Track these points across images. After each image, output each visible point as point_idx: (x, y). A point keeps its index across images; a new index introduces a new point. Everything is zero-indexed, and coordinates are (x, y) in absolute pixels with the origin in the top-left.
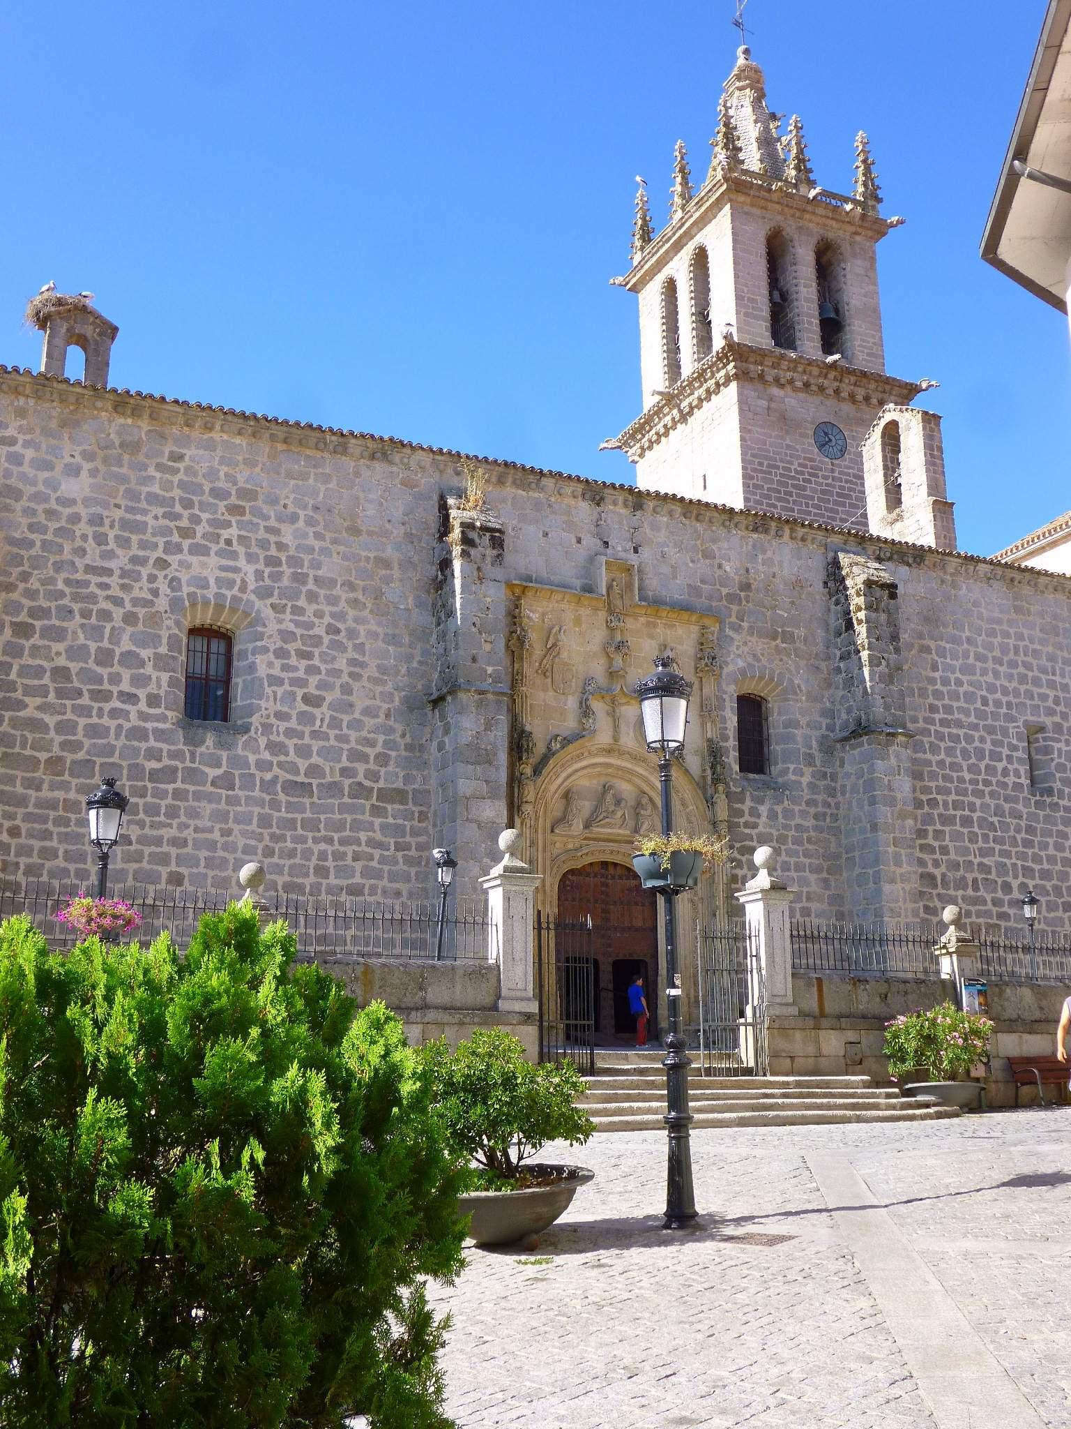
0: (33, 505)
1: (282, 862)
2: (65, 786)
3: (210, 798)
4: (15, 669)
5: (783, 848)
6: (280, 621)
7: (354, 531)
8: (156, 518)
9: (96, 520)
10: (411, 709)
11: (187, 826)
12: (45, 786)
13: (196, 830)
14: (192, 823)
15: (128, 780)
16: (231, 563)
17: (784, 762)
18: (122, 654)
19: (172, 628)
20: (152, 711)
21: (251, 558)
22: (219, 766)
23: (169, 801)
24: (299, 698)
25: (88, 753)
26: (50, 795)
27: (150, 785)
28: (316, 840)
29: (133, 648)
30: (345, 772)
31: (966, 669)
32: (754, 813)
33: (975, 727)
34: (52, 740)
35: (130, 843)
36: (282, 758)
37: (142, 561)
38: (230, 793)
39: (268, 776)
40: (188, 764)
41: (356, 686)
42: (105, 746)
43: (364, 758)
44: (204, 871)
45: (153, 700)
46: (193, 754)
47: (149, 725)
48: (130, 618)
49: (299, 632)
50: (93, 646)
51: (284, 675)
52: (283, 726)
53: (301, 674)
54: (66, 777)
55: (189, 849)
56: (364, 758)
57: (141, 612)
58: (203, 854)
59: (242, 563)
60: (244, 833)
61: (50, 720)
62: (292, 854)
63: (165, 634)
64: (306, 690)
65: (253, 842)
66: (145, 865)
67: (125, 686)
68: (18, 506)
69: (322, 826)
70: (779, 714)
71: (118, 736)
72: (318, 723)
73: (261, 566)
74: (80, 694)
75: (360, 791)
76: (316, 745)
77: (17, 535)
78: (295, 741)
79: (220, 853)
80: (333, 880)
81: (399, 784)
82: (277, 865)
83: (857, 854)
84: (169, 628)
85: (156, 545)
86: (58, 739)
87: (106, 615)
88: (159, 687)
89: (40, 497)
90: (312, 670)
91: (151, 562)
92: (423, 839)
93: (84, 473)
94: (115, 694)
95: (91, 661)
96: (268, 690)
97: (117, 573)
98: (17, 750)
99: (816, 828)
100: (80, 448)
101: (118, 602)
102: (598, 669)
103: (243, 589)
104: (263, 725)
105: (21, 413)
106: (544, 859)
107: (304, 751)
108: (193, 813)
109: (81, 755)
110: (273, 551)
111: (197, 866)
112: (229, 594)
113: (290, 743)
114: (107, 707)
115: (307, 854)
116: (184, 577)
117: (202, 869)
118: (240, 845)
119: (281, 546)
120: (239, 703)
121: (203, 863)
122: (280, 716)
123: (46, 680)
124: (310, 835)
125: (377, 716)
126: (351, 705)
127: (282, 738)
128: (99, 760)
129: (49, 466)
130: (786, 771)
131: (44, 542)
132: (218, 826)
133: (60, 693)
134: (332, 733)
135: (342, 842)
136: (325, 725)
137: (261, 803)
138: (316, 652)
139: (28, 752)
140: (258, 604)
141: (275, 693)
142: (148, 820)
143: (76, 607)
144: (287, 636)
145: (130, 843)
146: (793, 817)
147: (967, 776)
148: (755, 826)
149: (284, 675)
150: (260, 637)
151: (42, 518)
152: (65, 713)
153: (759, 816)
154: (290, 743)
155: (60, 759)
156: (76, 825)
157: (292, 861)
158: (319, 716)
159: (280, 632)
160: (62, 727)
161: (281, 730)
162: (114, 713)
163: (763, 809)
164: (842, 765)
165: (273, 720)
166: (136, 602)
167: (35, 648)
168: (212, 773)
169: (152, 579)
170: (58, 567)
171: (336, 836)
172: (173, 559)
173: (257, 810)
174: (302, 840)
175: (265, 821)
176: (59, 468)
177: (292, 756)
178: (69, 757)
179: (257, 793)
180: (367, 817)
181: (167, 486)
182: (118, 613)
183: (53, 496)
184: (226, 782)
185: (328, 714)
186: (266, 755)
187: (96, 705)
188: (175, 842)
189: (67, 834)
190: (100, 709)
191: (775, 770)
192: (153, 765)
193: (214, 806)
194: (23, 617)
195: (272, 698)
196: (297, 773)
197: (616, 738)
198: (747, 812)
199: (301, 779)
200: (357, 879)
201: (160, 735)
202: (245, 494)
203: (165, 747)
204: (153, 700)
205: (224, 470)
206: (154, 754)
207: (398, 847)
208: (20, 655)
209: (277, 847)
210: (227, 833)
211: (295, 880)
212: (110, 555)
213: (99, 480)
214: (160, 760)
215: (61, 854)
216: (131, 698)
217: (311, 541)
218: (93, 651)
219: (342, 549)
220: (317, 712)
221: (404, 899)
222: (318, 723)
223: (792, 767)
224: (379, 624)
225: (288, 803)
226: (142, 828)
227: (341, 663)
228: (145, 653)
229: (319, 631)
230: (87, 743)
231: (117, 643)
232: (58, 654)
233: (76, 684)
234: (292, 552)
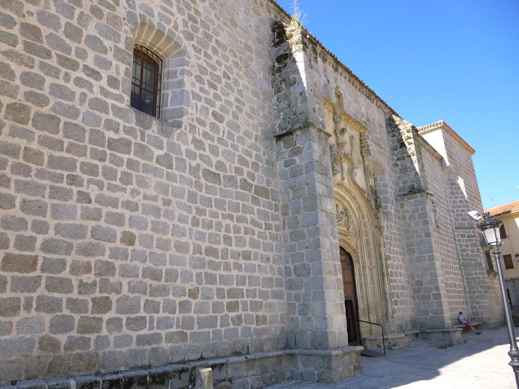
1: (204, 231)
2: (28, 135)
3: (156, 172)
6: (199, 59)
7: (235, 25)
10: (267, 138)
11: (138, 193)
13: (145, 197)
14: (142, 190)
15: (90, 142)
16: (168, 7)
18: (88, 36)
22: (162, 149)
23: (124, 168)
24: (210, 113)
25: (53, 109)
26: (10, 140)
27: (108, 152)
29: (98, 36)
34: (17, 87)
35: (90, 202)
38: (169, 170)
39: (194, 164)
40: (139, 141)
41: (240, 115)
42: (70, 107)
43: (246, 163)
44: (151, 233)
45: (113, 82)
46: (143, 134)
47: (110, 101)
49: (209, 70)
52: (202, 129)
54: (29, 126)
55: (139, 213)
58: (150, 218)
59: (174, 10)
60: (180, 205)
61: (18, 69)
62: (209, 226)
64: (214, 109)
65: (185, 213)
66: (102, 223)
67: (90, 62)
69: (226, 207)
70: (381, 180)
72: (221, 133)
74: (49, 55)
75: (246, 185)
76: (221, 148)
78: (209, 142)
79: (163, 219)
80: (234, 248)
81: (264, 185)
82: (201, 233)
84: (126, 32)
86: (24, 89)
88: (118, 73)
94: (81, 67)
96: (192, 101)
103: (176, 27)
104: (190, 125)
107: (214, 150)
108: (142, 183)
109: (46, 110)
111: (146, 228)
112: (167, 27)
113: (207, 143)
114: (74, 74)
115: (219, 226)
117: (149, 232)
118: (177, 215)
120: (169, 107)
121: (150, 225)
122: (202, 123)
127: (201, 138)
132: (160, 196)
135: (239, 220)
136: (225, 136)
137: (190, 183)
140: (185, 42)
141: (197, 105)
142: (106, 182)
145: (90, 202)
150: (186, 63)
152: (32, 67)
154: (207, 143)
155: (24, 108)
156: (37, 175)
157: (210, 231)
158: (221, 128)
161: (201, 132)
162: (79, 81)
165: (195, 123)
168: (157, 152)
173: (187, 188)
175: (192, 198)
177: (207, 153)
178: (34, 109)
179: (187, 175)
186: (192, 147)
187: (64, 70)
188: (128, 205)
189: (26, 183)
192: (110, 134)
193: (158, 179)
195: (195, 108)
196: (211, 166)
199: (213, 169)
200: (247, 248)
201: (117, 111)
203: (122, 122)
204: (113, 82)
206: (111, 126)
209: (201, 218)
210: (167, 203)
211: (213, 245)
214: (117, 132)
215: (18, 202)
216: (96, 75)
221: (271, 263)
222: (221, 133)
224: (249, 82)
225: (207, 186)
226: (101, 188)
229: (220, 73)
230: (53, 101)
231: (86, 26)
232: (30, 13)
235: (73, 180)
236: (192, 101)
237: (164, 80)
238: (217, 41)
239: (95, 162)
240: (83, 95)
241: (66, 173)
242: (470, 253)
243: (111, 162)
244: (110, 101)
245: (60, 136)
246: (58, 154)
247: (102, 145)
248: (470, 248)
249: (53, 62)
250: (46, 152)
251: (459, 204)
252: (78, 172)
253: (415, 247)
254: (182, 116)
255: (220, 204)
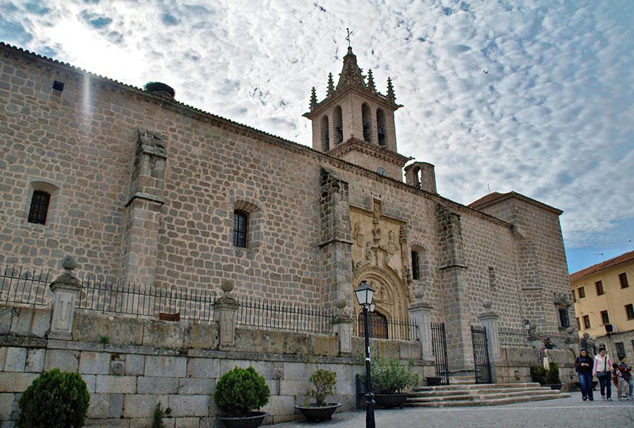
0: (181, 156)
2: (193, 270)
3: (246, 278)
4: (174, 220)
6: (268, 211)
8: (225, 166)
9: (204, 164)
12: (185, 269)
13: (240, 291)
14: (239, 288)
19: (230, 210)
20: (223, 242)
21: (258, 185)
22: (248, 266)
25: (201, 257)
27: (223, 272)
28: (282, 297)
29: (217, 216)
30: (292, 271)
31: (473, 247)
33: (476, 267)
36: (270, 264)
37: (221, 182)
39: (265, 271)
41: (294, 238)
43: (297, 266)
45: (224, 237)
46: (239, 260)
48: (216, 204)
49: (275, 215)
50: (203, 214)
51: (270, 231)
52: (270, 251)
53: (276, 232)
54: (193, 266)
56: (297, 266)
57: (220, 202)
59: (255, 186)
60: (258, 293)
61: (187, 242)
63: (228, 212)
67: (214, 231)
68: (176, 156)
71: (211, 251)
73: (261, 189)
75: (296, 279)
77: (175, 167)
78: (274, 257)
83: (449, 309)
85: (225, 177)
86: (190, 250)
87: (207, 202)
88: (226, 232)
89: (183, 153)
90: (280, 230)
91: (223, 183)
92: (318, 298)
93: (200, 145)
95: (202, 220)
96: (265, 237)
97: (211, 186)
98: (175, 254)
99: (436, 300)
100: (198, 136)
101: (211, 197)
102: (371, 238)
103: (255, 197)
105: (178, 120)
107: (277, 262)
109: (198, 258)
110: (265, 184)
113: (273, 259)
114: (208, 239)
116: (235, 190)
119: (268, 182)
122: (270, 248)
123: (185, 226)
124: (280, 295)
125: (301, 250)
126: (293, 245)
127: (270, 256)
128: (205, 261)
129: (187, 142)
130: (426, 279)
131: (185, 170)
133: (191, 232)
134: (287, 255)
135: (291, 298)
137: (263, 281)
138: (281, 223)
139: (178, 255)
140: (261, 203)
141: (267, 238)
143: (196, 197)
144: (271, 217)
147: (475, 284)
149: (270, 231)
151: (184, 161)
154: (273, 259)
159: (268, 215)
160: (192, 246)
162: (211, 242)
164: (442, 278)
166: (218, 198)
167: (181, 213)
169: (224, 189)
170: (190, 181)
171: (289, 296)
172: (232, 183)
173: (261, 284)
174: (277, 297)
175: (264, 289)
176: (191, 142)
177: (273, 264)
178: (194, 258)
180: (299, 289)
181: (229, 154)
182: (211, 202)
183: (189, 153)
184: (250, 272)
185: (285, 248)
186: (264, 263)
187: (204, 238)
190: (205, 239)
194: (177, 200)
197: (377, 265)
199: (276, 273)
201: (227, 252)
202: (255, 160)
204: (224, 237)
205: (249, 151)
206: (225, 259)
207: (311, 301)
208: (176, 215)
210: (251, 293)
212: (208, 178)
213: (205, 149)
214: (227, 262)
216: (217, 236)
217: (278, 181)
218: (202, 216)
219: (288, 185)
220: (281, 247)
227: (289, 228)
228: (221, 219)
233: (197, 229)
234: (272, 185)
235: (210, 286)
236: (265, 237)
237: (250, 226)
238: (280, 196)
239: (218, 277)
240: (212, 247)
241: (207, 284)
242: (534, 311)
243: (225, 276)
244: (223, 247)
245: (204, 268)
246: (203, 276)
247: (220, 269)
248: (535, 307)
249: (199, 236)
250: (199, 276)
251: (527, 267)
252: (211, 283)
253: (449, 309)
254: (259, 246)
255: (280, 291)
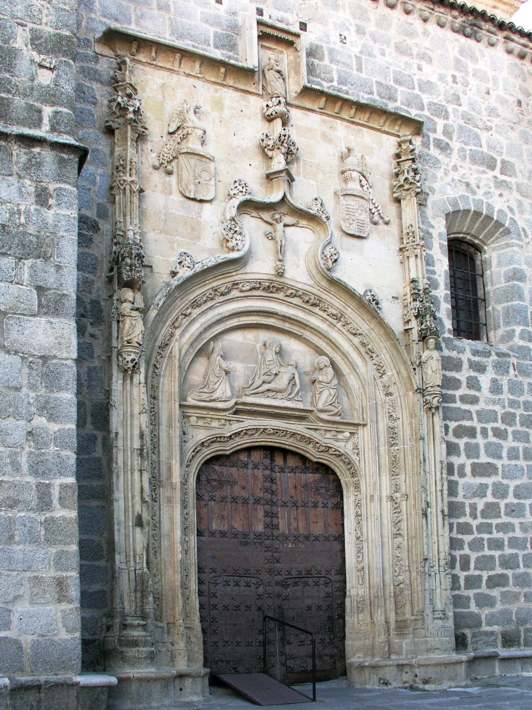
5: (510, 429)
17: (507, 323)
32: (473, 384)
70: (499, 264)
106: (169, 437)
130: (510, 335)
146: (521, 392)
148: (474, 400)
153: (479, 389)
163: (485, 380)
191: (495, 335)
198: (464, 384)
223: (518, 329)
